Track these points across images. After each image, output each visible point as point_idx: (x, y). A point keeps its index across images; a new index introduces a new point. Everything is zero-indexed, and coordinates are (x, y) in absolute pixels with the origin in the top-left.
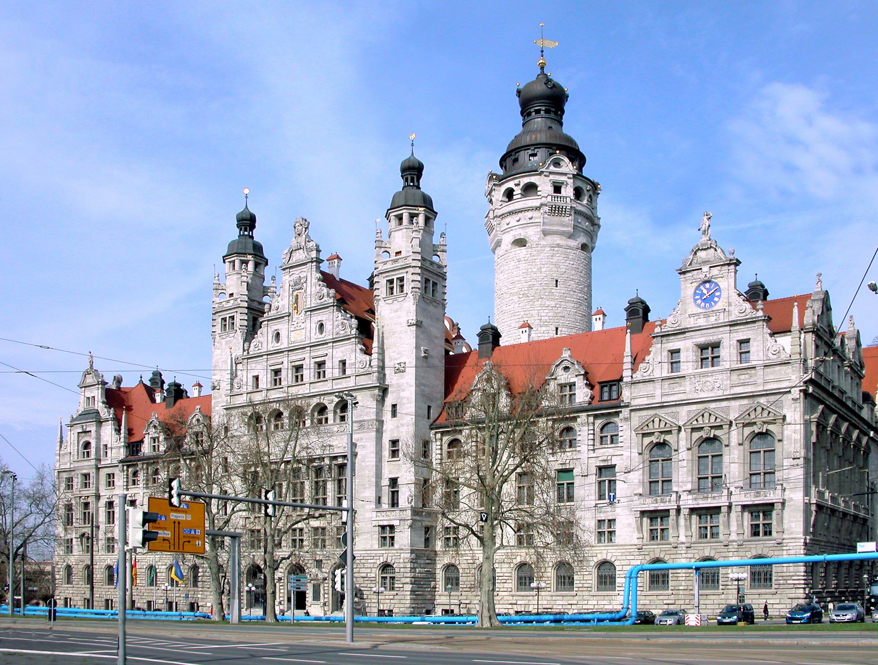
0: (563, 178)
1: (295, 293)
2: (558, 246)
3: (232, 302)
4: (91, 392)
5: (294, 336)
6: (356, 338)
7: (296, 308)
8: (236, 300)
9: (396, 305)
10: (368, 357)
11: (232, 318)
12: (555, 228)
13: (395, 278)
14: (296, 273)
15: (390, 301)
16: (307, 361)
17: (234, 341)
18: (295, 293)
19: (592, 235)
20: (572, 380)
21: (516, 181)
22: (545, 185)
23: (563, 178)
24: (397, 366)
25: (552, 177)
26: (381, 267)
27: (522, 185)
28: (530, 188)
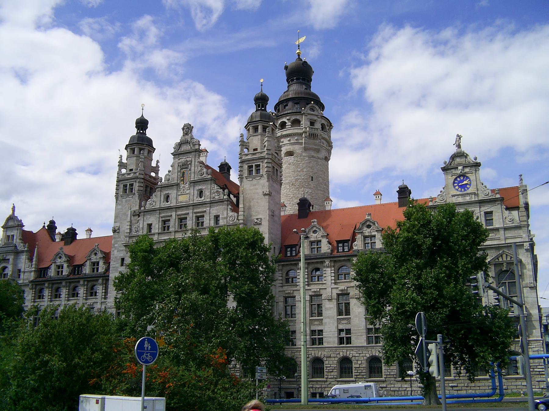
0: (315, 118)
1: (182, 171)
2: (313, 157)
3: (132, 174)
4: (12, 231)
5: (182, 198)
6: (227, 201)
7: (183, 180)
8: (135, 173)
9: (255, 181)
10: (236, 214)
11: (132, 185)
12: (311, 146)
13: (254, 165)
14: (183, 159)
15: (251, 179)
16: (191, 215)
17: (132, 200)
18: (182, 171)
19: (329, 153)
20: (373, 234)
21: (288, 118)
22: (305, 122)
23: (315, 118)
24: (256, 221)
25: (309, 117)
26: (244, 158)
27: (291, 121)
28: (296, 123)
